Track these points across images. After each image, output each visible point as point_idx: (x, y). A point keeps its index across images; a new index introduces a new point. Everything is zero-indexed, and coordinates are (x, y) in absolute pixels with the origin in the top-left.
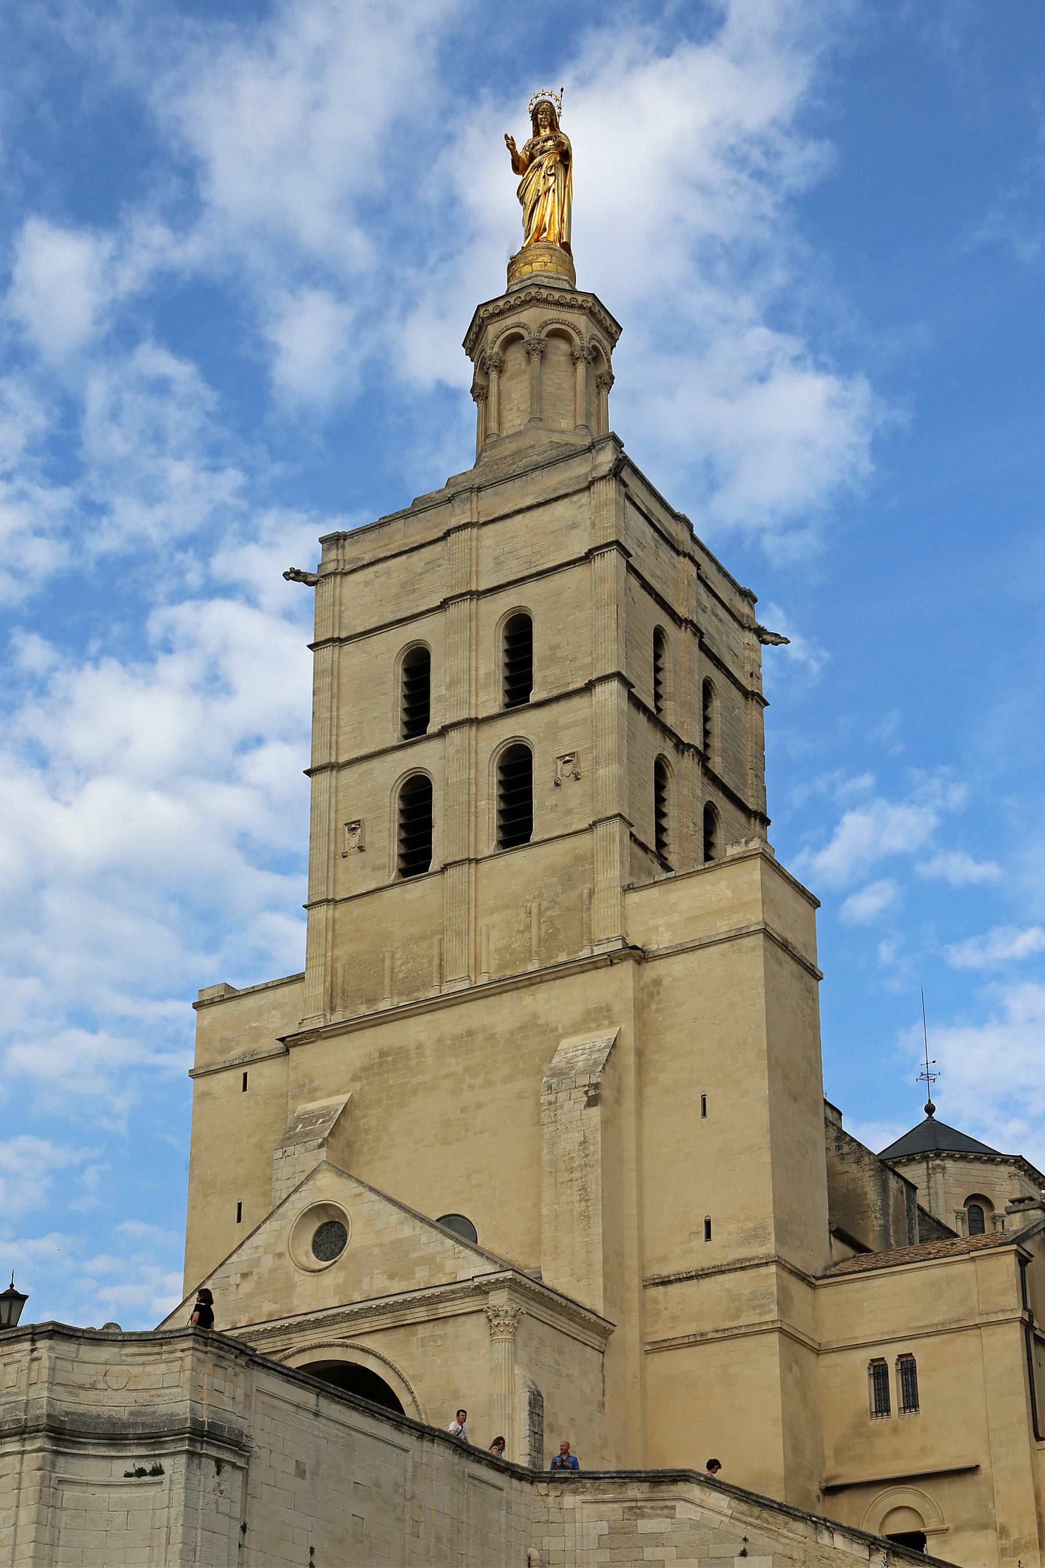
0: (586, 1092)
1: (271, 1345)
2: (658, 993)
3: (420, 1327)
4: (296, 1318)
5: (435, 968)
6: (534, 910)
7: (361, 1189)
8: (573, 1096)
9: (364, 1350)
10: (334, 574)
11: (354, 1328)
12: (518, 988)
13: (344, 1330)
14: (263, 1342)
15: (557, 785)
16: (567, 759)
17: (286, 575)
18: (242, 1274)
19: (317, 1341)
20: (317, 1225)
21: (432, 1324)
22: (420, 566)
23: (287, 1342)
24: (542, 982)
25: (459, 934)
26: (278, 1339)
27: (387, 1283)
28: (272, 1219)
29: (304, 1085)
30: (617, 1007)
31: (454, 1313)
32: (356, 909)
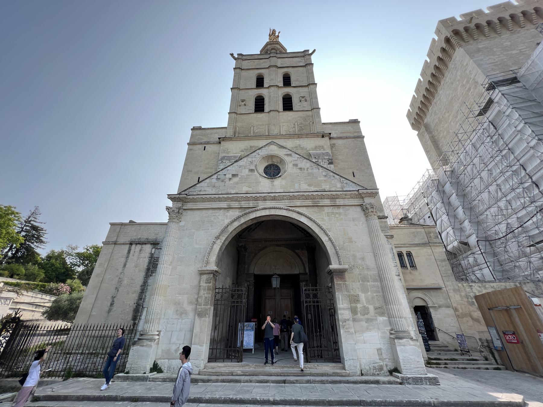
0: (328, 161)
1: (247, 204)
2: (335, 147)
3: (325, 208)
4: (263, 194)
5: (267, 131)
6: (296, 124)
7: (290, 153)
8: (324, 161)
9: (299, 213)
10: (241, 59)
11: (292, 203)
12: (294, 138)
13: (287, 203)
14: (243, 202)
15: (300, 101)
16: (303, 97)
17: (230, 54)
18: (232, 175)
19: (271, 206)
20: (266, 164)
21: (332, 207)
22: (262, 62)
23: (256, 204)
24: (302, 138)
25: (274, 125)
26: (251, 202)
27: (308, 187)
28: (249, 157)
29: (225, 150)
30: (325, 147)
31: (344, 204)
32: (243, 117)
